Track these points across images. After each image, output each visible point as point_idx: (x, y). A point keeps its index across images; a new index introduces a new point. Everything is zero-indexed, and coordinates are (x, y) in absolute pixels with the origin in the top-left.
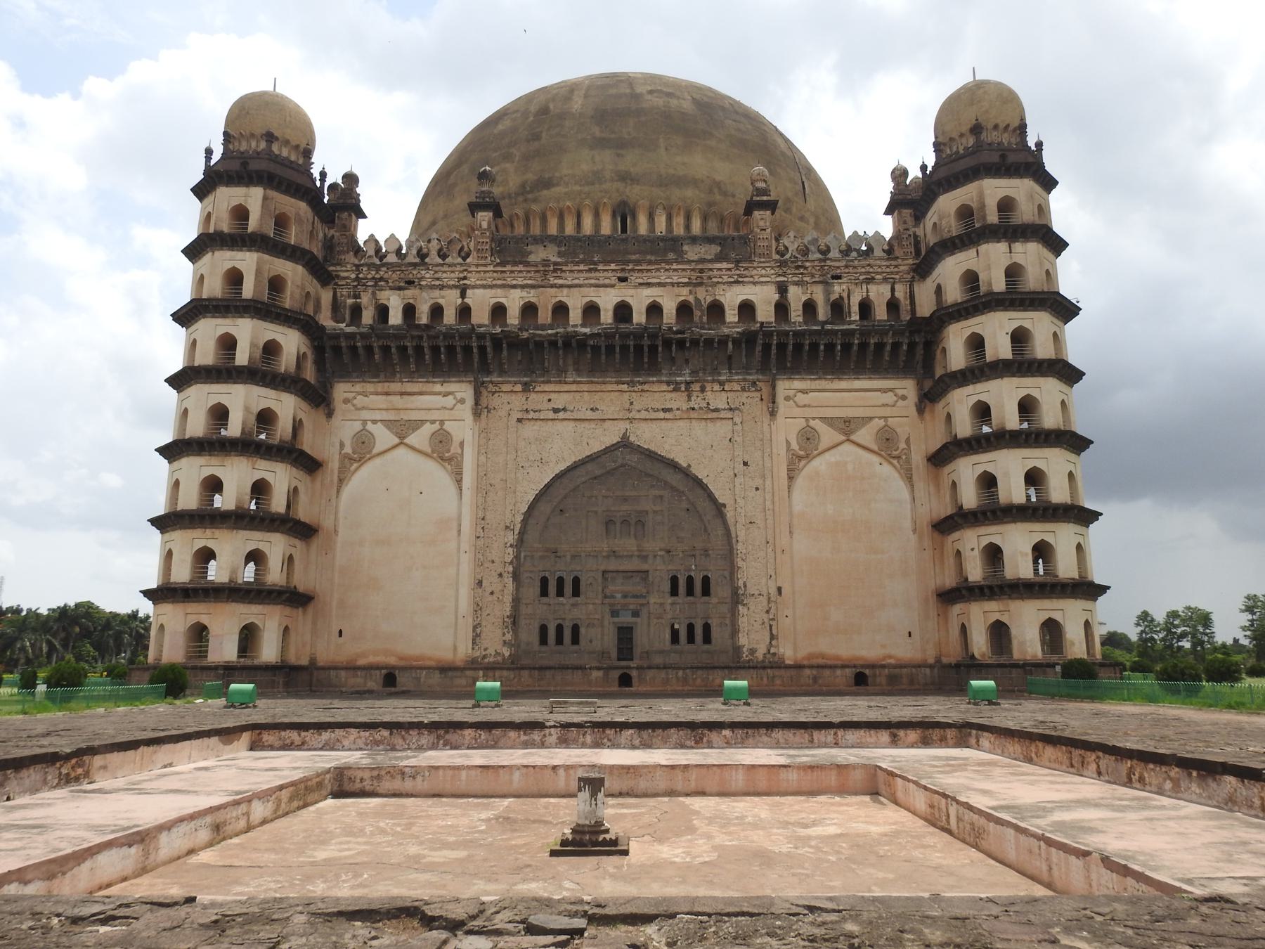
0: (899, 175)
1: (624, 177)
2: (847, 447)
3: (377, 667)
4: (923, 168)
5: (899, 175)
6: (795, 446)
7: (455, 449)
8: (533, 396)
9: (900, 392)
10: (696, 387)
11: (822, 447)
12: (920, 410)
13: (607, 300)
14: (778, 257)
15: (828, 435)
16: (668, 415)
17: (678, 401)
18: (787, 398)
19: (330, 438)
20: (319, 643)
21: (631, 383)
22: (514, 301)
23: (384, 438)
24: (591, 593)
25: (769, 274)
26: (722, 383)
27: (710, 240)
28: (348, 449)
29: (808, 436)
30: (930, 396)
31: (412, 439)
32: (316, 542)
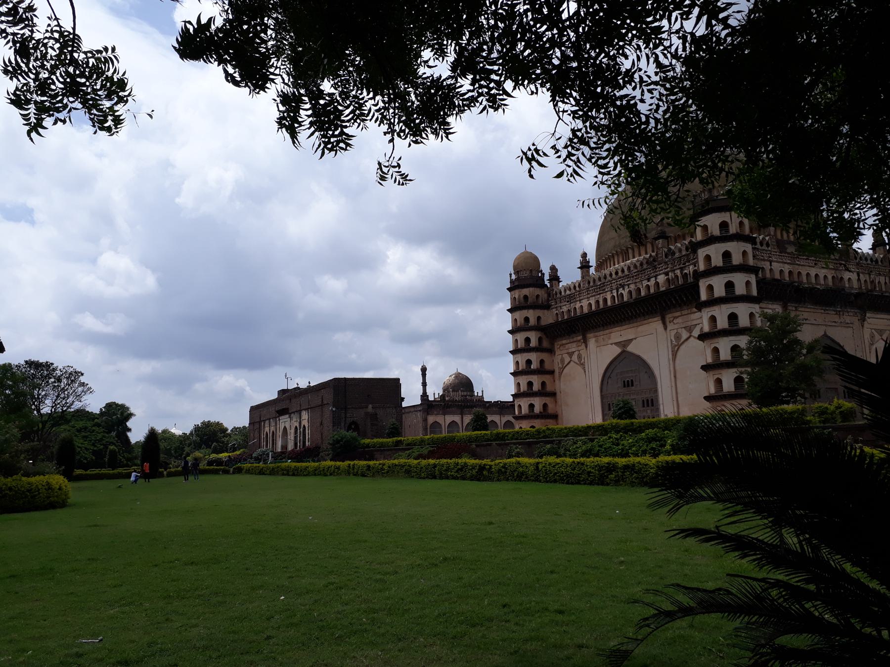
11: (682, 340)
15: (685, 335)
19: (555, 362)
28: (560, 366)
29: (678, 337)
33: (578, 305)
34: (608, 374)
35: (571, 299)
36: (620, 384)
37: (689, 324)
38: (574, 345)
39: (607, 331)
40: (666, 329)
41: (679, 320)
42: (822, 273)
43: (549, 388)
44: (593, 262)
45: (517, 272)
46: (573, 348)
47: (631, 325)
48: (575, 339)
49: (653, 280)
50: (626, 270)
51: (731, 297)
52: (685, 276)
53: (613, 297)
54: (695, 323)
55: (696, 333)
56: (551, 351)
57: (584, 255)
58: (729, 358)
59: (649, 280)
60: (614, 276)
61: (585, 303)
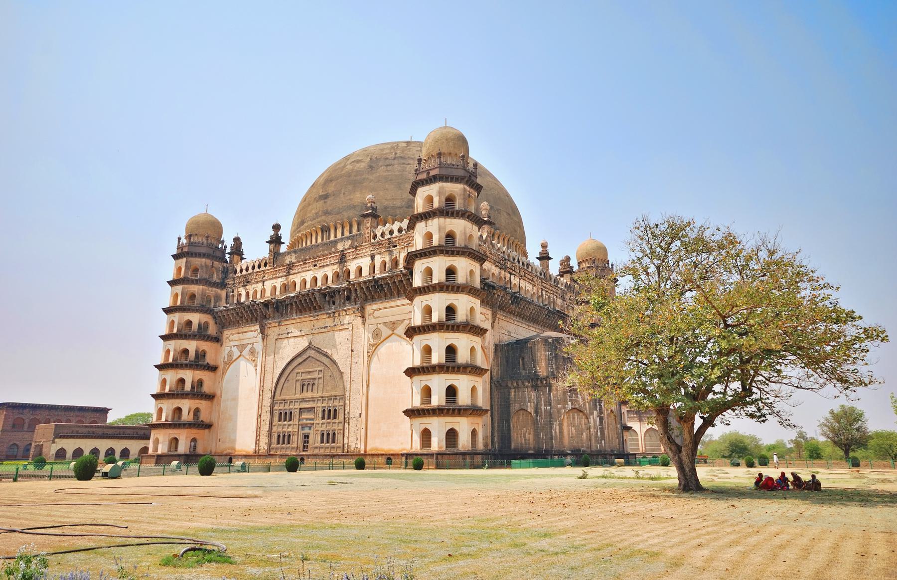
1: (326, 213)
3: (226, 455)
8: (282, 327)
10: (336, 314)
13: (308, 276)
14: (373, 241)
15: (385, 331)
16: (326, 330)
17: (329, 322)
18: (370, 315)
20: (206, 443)
21: (314, 316)
23: (236, 353)
25: (368, 251)
26: (346, 311)
27: (348, 238)
32: (215, 400)
42: (529, 287)
43: (206, 389)
44: (286, 236)
45: (189, 237)
51: (450, 284)
55: (401, 330)
56: (217, 340)
57: (277, 227)
58: (443, 361)
61: (269, 285)
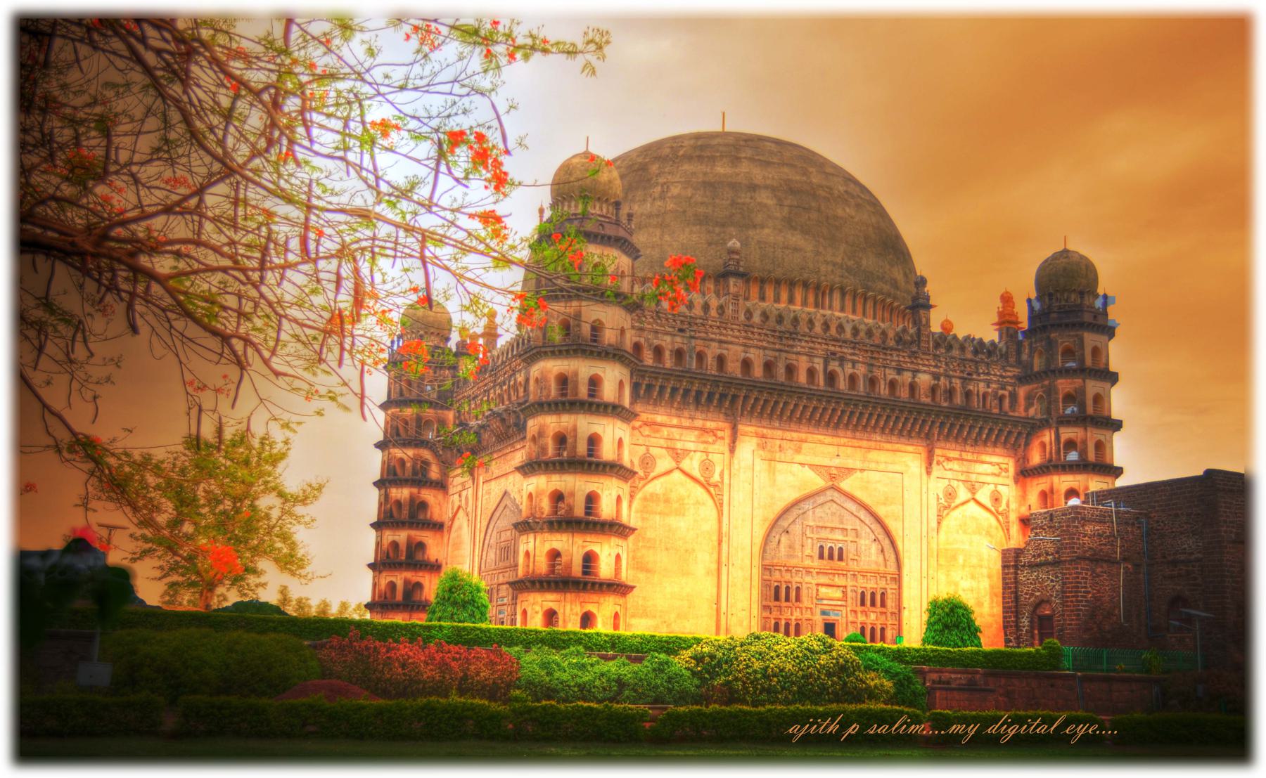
0: (1007, 299)
2: (972, 504)
4: (1029, 301)
5: (1007, 299)
6: (943, 501)
7: (716, 478)
9: (1004, 466)
11: (958, 501)
12: (1016, 481)
15: (963, 494)
18: (938, 463)
22: (757, 358)
23: (665, 463)
24: (806, 602)
29: (951, 495)
30: (1025, 474)
31: (685, 464)
33: (712, 351)
34: (784, 523)
35: (685, 326)
36: (811, 549)
37: (973, 477)
38: (692, 435)
39: (795, 435)
40: (929, 473)
41: (955, 465)
46: (688, 440)
47: (856, 443)
48: (698, 423)
49: (907, 376)
50: (848, 329)
52: (968, 394)
53: (811, 373)
54: (983, 478)
55: (984, 495)
59: (900, 371)
60: (818, 329)
